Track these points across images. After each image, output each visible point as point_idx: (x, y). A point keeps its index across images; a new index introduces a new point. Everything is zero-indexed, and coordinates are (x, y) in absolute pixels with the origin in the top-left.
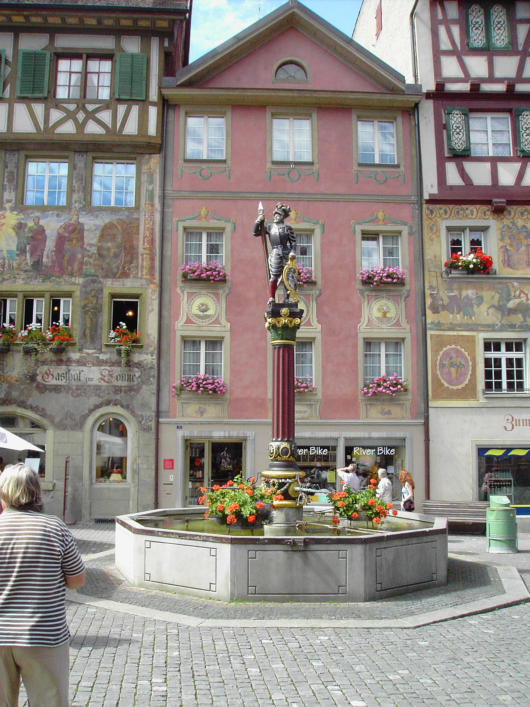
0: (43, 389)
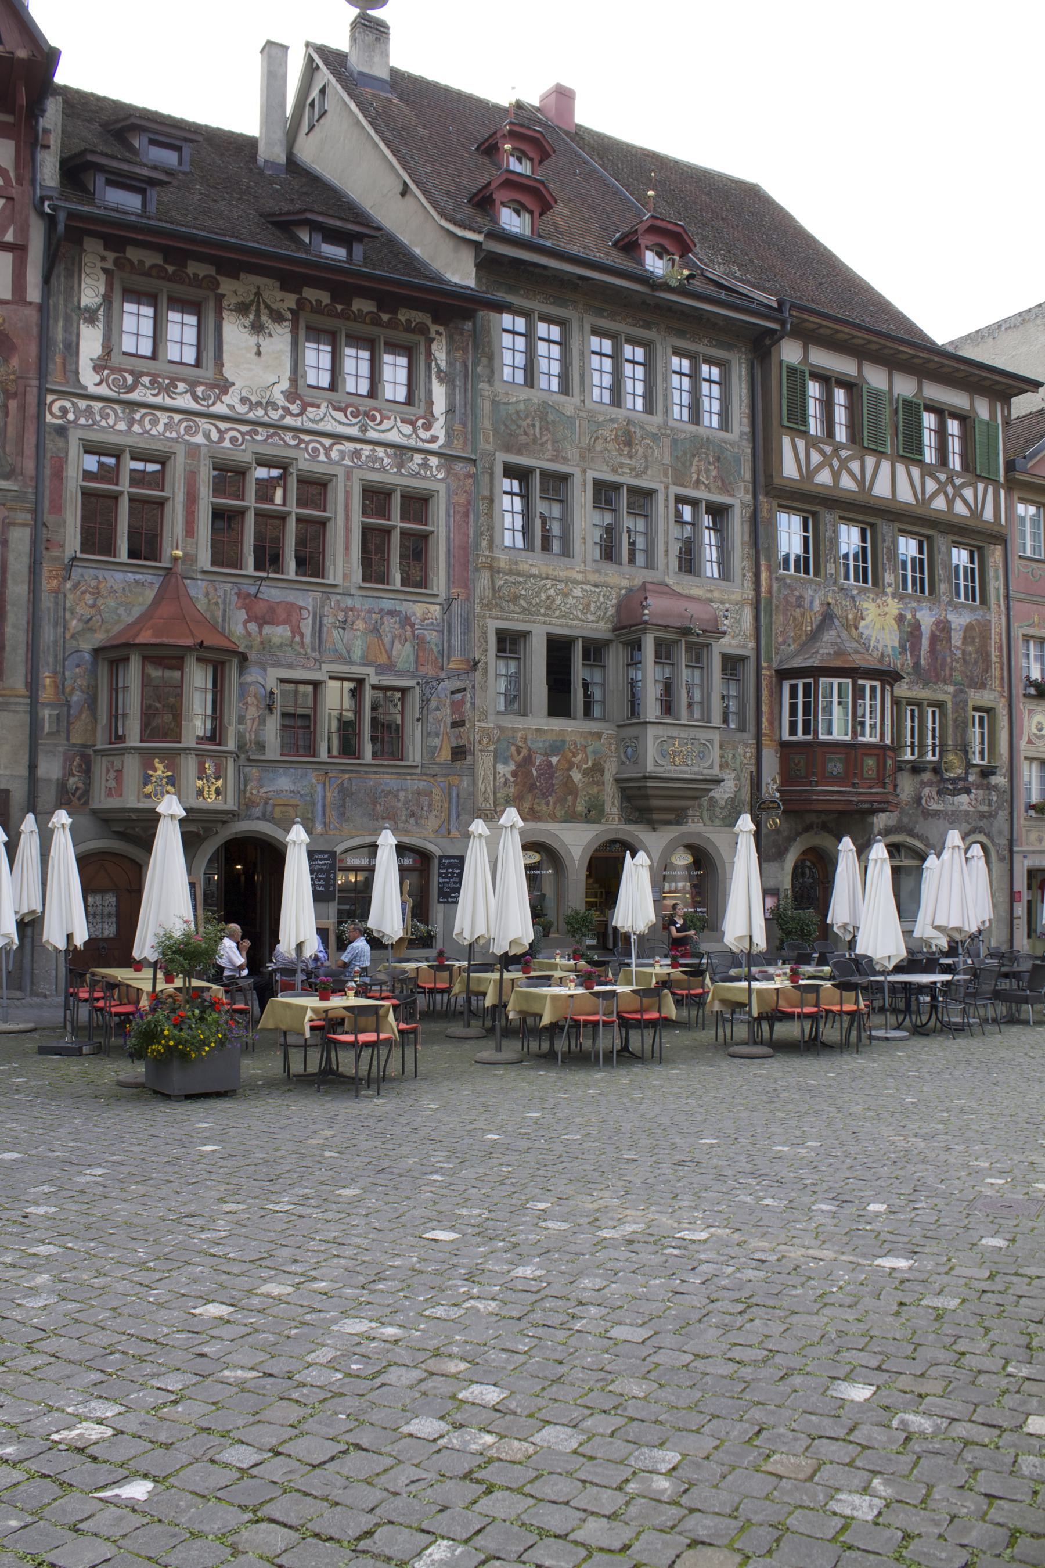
0: (927, 814)
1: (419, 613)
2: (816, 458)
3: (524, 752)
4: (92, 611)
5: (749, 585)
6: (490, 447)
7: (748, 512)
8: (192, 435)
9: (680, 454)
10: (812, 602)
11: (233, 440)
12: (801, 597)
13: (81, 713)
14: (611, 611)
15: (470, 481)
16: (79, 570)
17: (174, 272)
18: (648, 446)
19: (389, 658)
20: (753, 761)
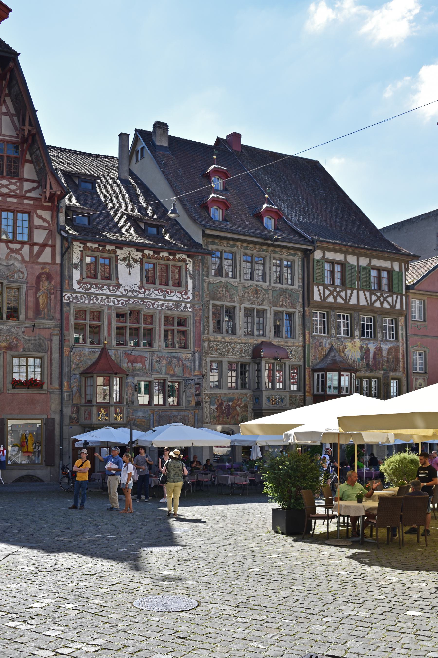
1: (184, 357)
2: (327, 292)
3: (220, 401)
4: (79, 362)
5: (301, 339)
6: (208, 299)
7: (301, 314)
8: (109, 303)
10: (326, 344)
11: (122, 303)
12: (322, 342)
13: (76, 394)
14: (250, 352)
15: (201, 311)
17: (102, 249)
18: (264, 294)
20: (303, 402)
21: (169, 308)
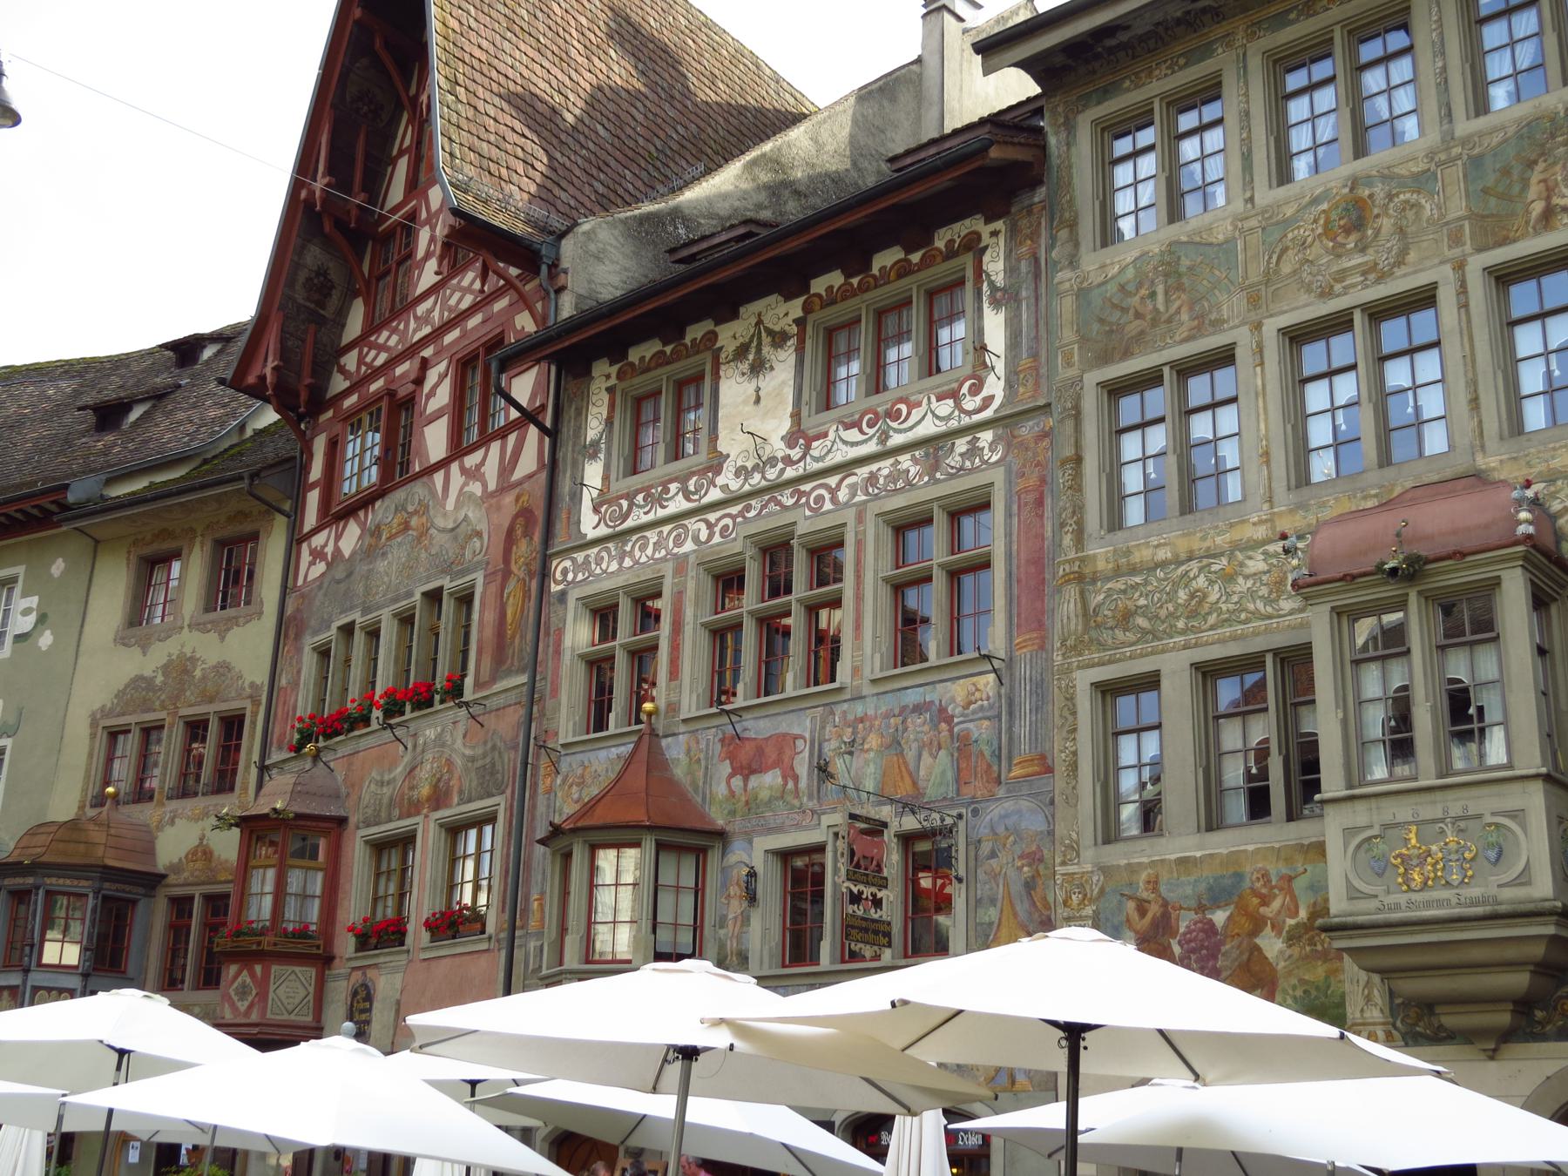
3: (1154, 910)
6: (1073, 372)
9: (1490, 179)
16: (568, 759)
19: (915, 784)
21: (900, 484)
